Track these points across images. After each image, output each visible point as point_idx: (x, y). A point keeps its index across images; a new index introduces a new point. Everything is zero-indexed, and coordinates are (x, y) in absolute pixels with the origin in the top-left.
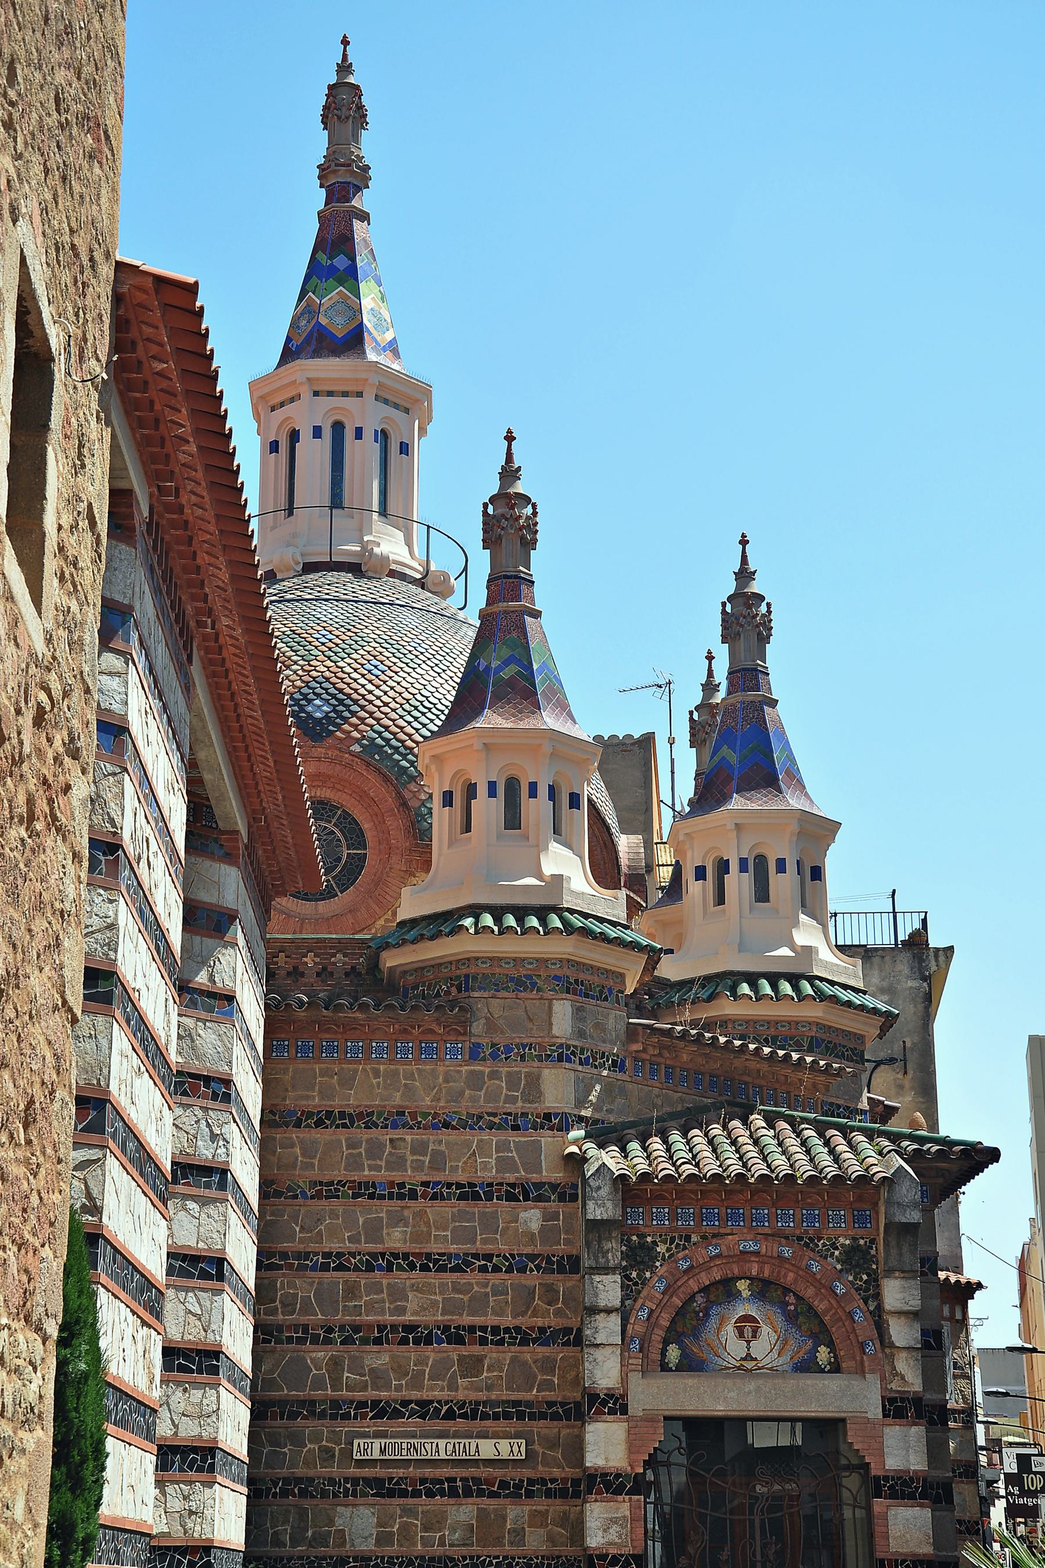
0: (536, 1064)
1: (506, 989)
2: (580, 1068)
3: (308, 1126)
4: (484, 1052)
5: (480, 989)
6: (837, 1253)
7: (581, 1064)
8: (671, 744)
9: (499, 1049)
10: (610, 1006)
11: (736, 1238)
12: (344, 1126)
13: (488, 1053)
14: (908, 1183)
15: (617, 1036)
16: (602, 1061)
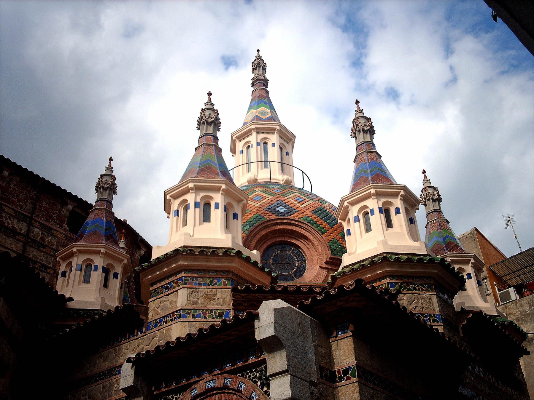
0: (171, 323)
1: (162, 293)
2: (192, 320)
3: (92, 383)
4: (152, 326)
5: (153, 297)
6: (258, 375)
7: (194, 317)
8: (516, 238)
9: (157, 322)
10: (218, 287)
11: (204, 381)
12: (103, 379)
13: (153, 326)
14: (267, 312)
15: (224, 301)
16: (211, 314)
